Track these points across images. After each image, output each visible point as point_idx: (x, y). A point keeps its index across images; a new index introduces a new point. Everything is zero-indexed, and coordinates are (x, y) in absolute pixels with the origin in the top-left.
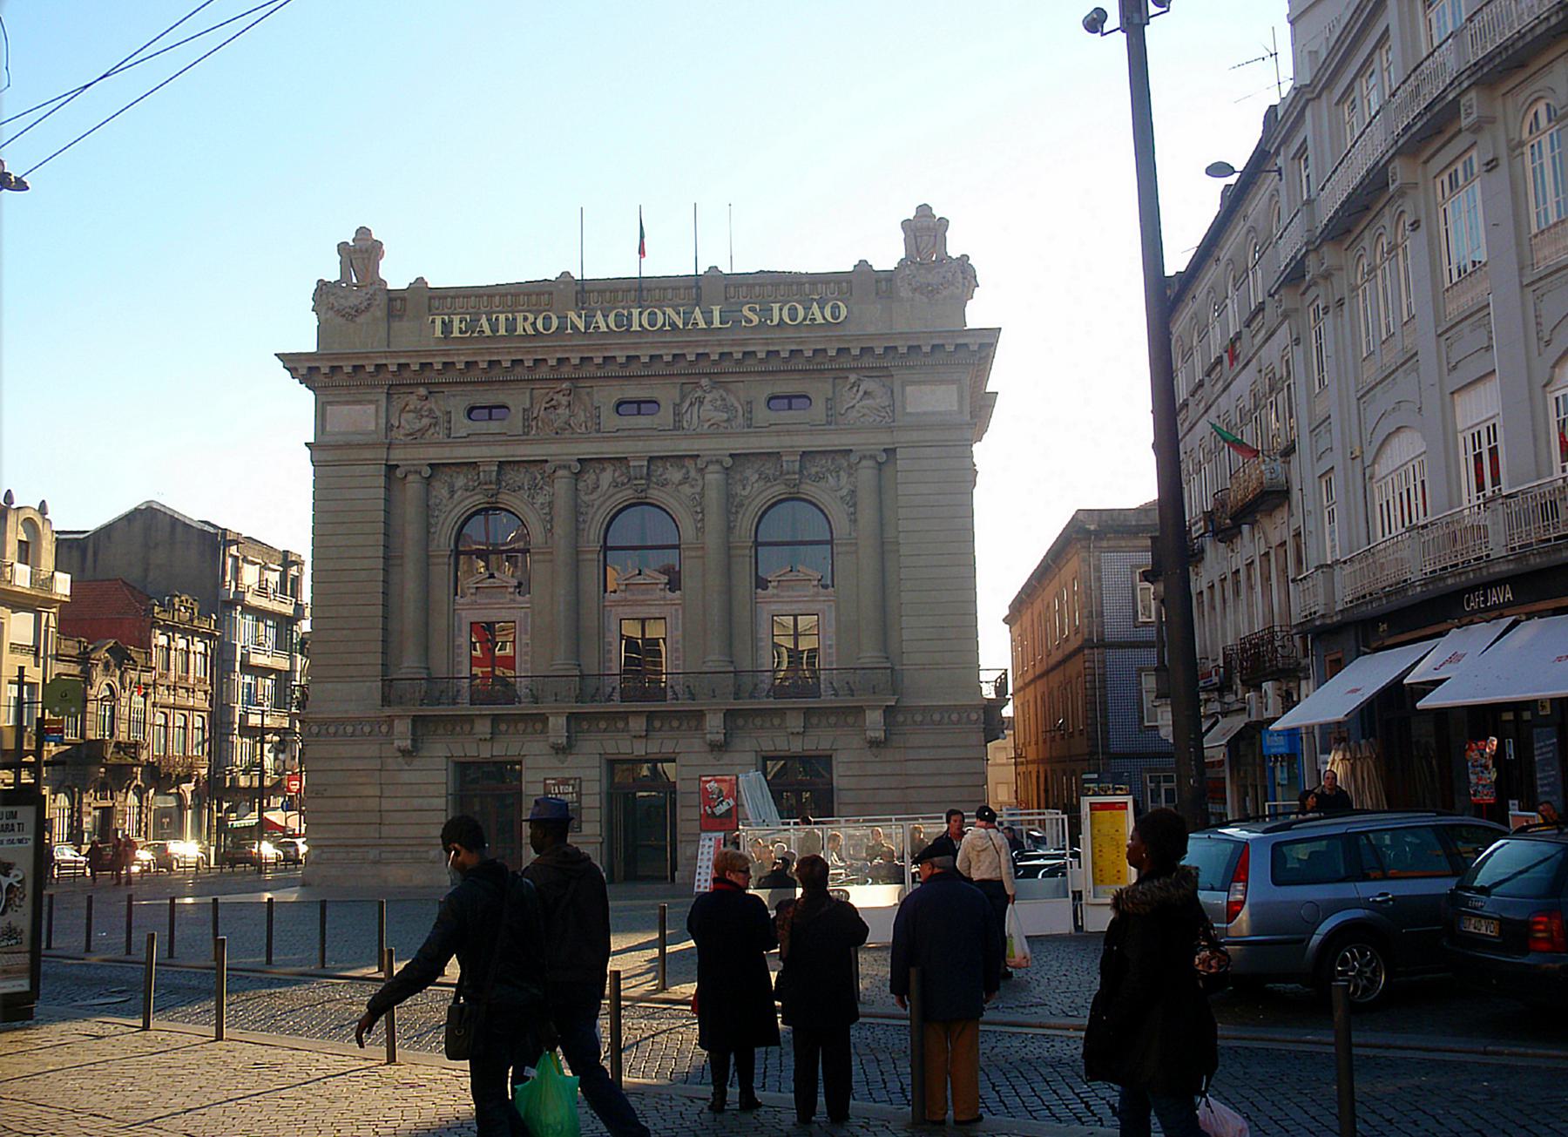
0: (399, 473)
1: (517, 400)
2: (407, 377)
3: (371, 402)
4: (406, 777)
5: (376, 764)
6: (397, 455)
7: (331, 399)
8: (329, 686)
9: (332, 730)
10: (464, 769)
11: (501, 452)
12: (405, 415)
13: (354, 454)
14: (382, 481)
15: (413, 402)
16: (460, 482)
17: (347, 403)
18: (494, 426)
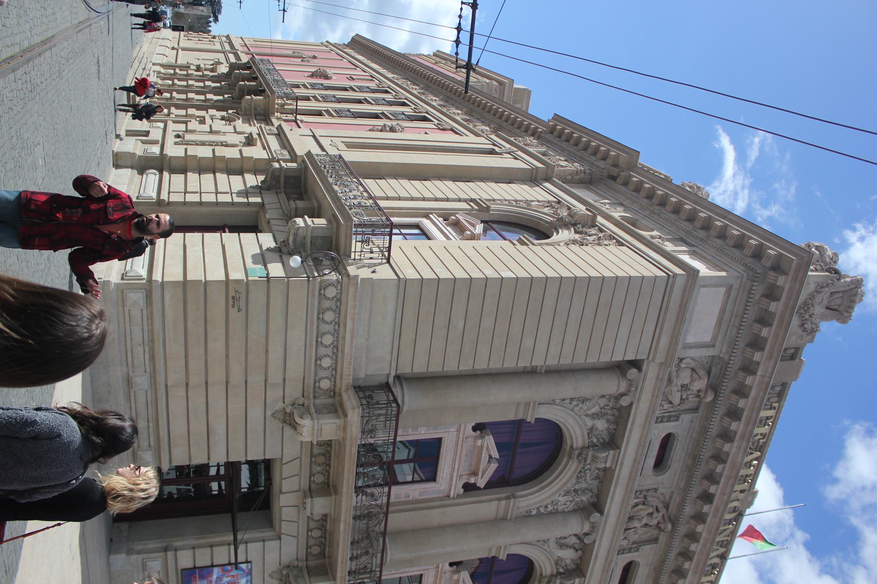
0: (633, 372)
1: (668, 481)
2: (729, 385)
3: (715, 337)
4: (256, 414)
5: (275, 375)
6: (651, 371)
7: (733, 293)
8: (391, 307)
9: (329, 316)
10: (263, 469)
11: (624, 472)
12: (688, 372)
13: (668, 325)
14: (630, 357)
15: (700, 384)
16: (601, 425)
17: (723, 311)
18: (651, 461)
